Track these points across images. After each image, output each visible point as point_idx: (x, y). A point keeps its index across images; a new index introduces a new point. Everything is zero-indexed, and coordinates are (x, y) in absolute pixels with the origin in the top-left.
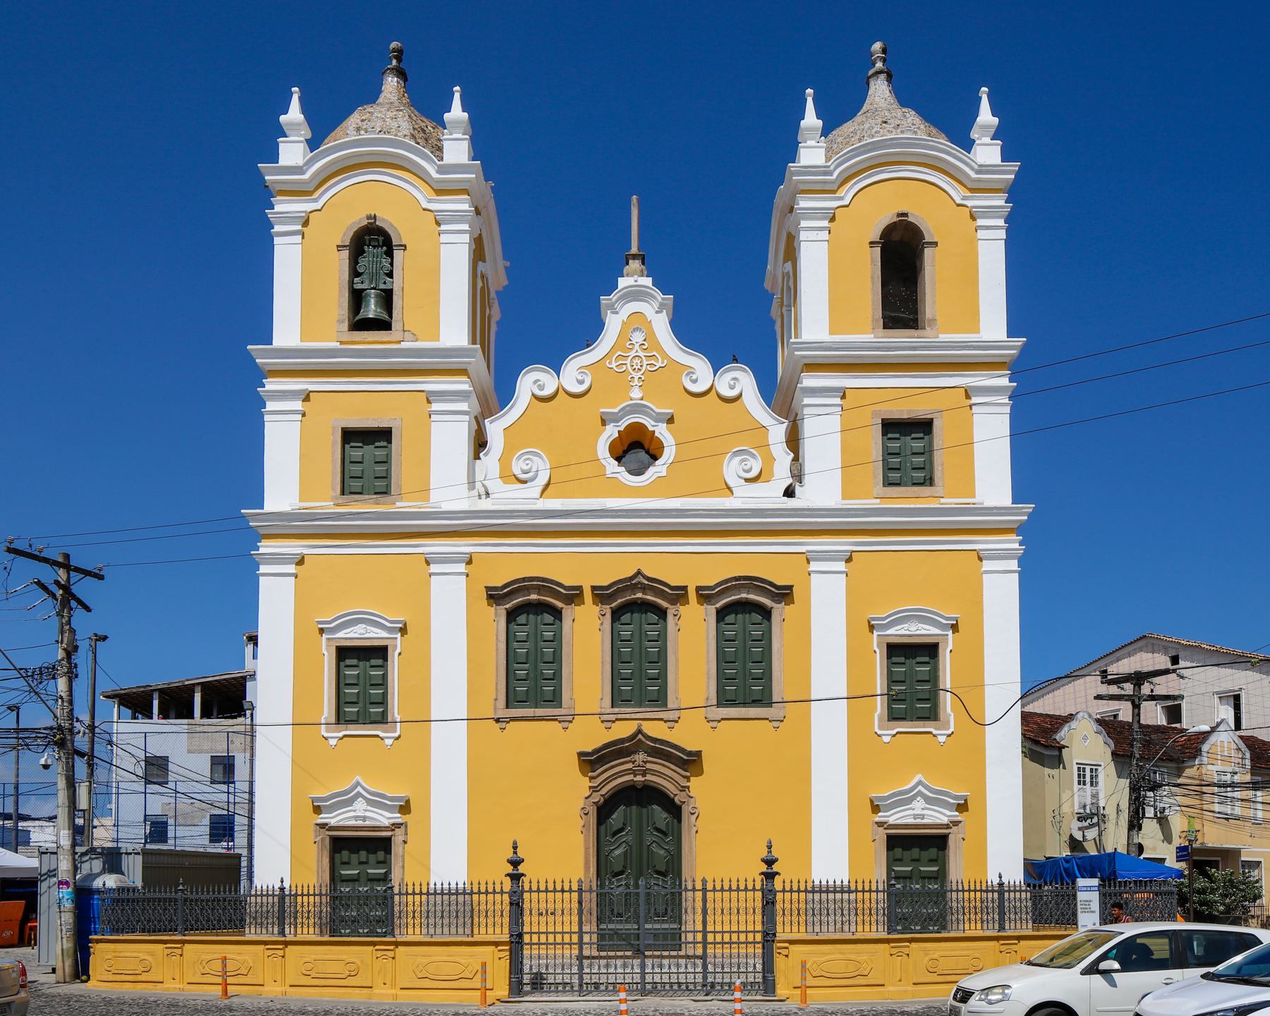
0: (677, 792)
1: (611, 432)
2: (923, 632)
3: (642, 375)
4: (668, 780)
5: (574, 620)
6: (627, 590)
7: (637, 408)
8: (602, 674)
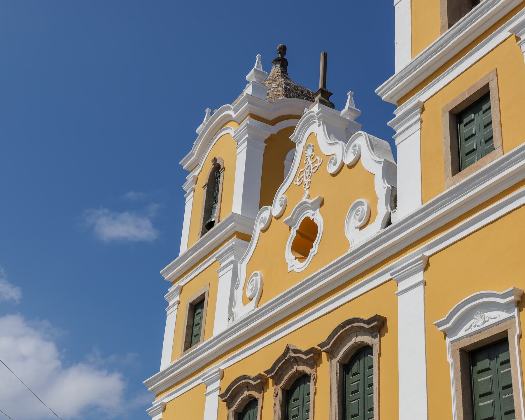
1: (293, 233)
2: (491, 322)
3: (310, 179)
7: (303, 207)
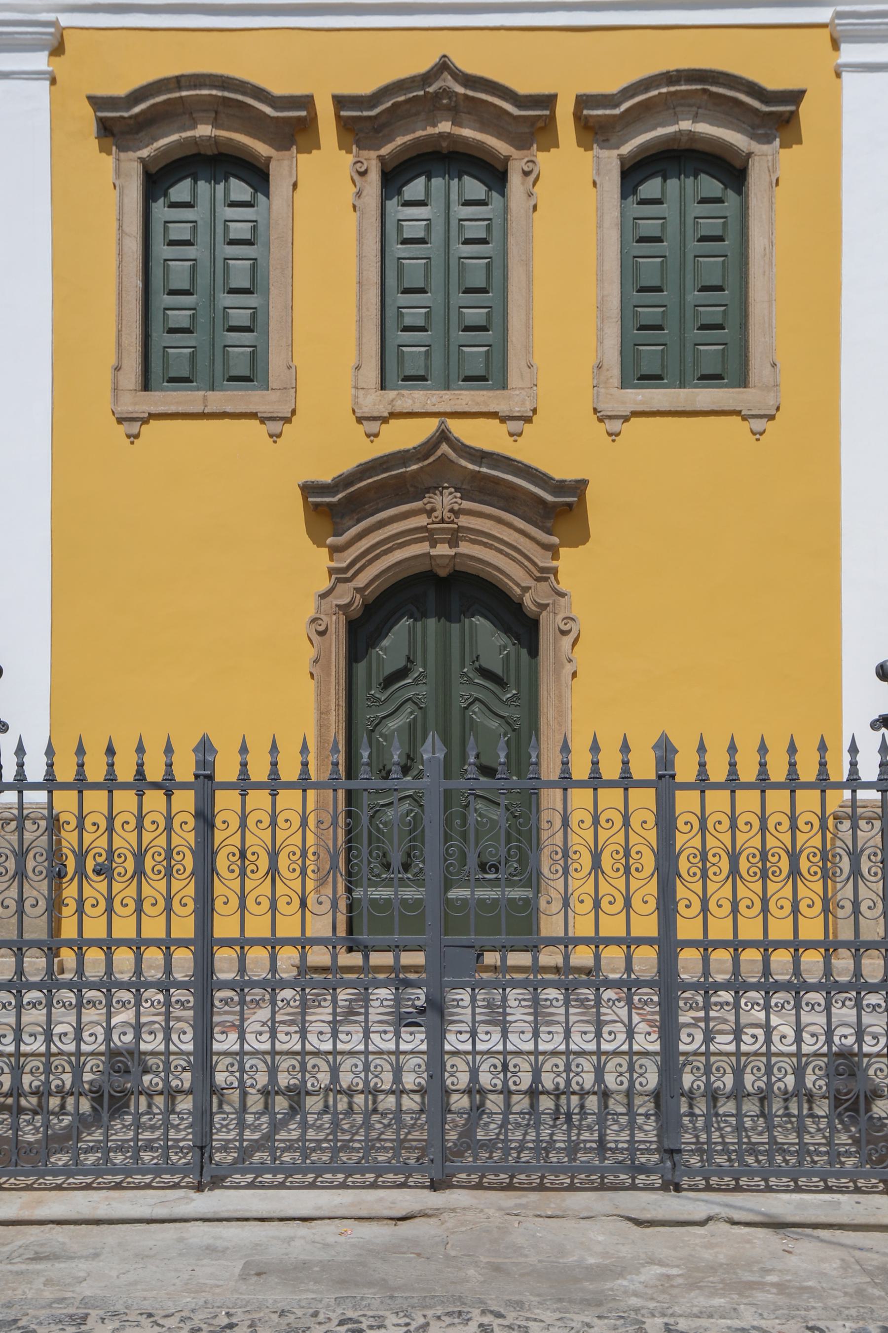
0: (527, 582)
4: (507, 555)
5: (295, 185)
6: (417, 114)
8: (359, 309)
